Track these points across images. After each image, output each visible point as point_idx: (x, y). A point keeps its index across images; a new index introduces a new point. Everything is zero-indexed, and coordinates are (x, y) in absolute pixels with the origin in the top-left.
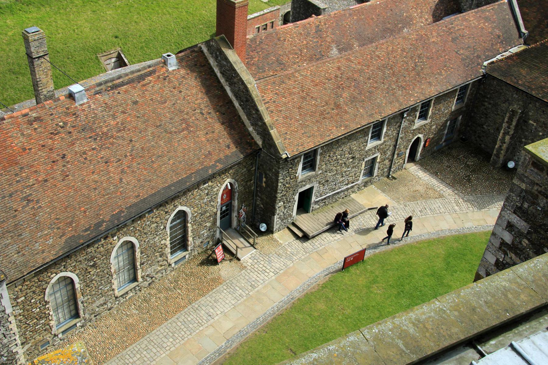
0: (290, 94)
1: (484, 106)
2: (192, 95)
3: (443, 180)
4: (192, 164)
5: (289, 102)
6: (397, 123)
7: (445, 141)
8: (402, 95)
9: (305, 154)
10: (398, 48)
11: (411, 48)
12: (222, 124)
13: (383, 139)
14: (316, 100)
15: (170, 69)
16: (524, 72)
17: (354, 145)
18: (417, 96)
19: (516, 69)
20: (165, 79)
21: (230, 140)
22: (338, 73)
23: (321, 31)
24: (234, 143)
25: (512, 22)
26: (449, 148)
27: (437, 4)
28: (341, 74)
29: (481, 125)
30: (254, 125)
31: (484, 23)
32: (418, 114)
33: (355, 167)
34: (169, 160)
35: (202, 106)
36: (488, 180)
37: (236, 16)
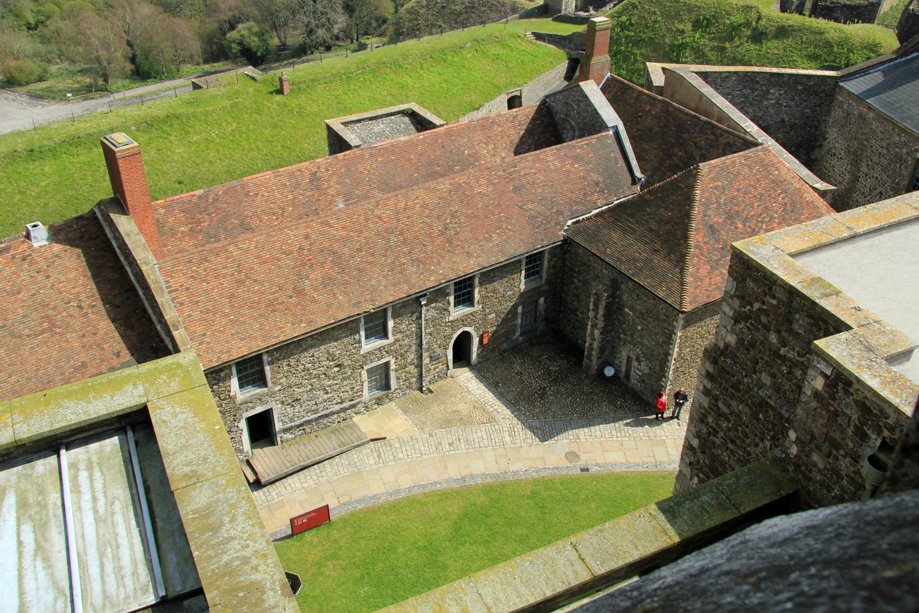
0: (217, 277)
1: (574, 283)
2: (69, 280)
3: (501, 396)
4: (49, 382)
5: (213, 289)
6: (413, 313)
7: (521, 335)
8: (416, 273)
9: (238, 364)
10: (416, 204)
11: (439, 203)
12: (113, 322)
13: (391, 339)
14: (261, 283)
15: (36, 245)
16: (615, 236)
17: (335, 347)
18: (442, 274)
19: (605, 231)
20: (24, 260)
21: (123, 345)
22: (306, 244)
23: (319, 180)
24: (129, 349)
25: (621, 162)
26: (531, 345)
27: (523, 137)
28: (311, 245)
29: (574, 311)
30: (160, 322)
32: (452, 299)
33: (349, 378)
34: (10, 376)
35: (83, 297)
36: (568, 395)
37: (121, 169)
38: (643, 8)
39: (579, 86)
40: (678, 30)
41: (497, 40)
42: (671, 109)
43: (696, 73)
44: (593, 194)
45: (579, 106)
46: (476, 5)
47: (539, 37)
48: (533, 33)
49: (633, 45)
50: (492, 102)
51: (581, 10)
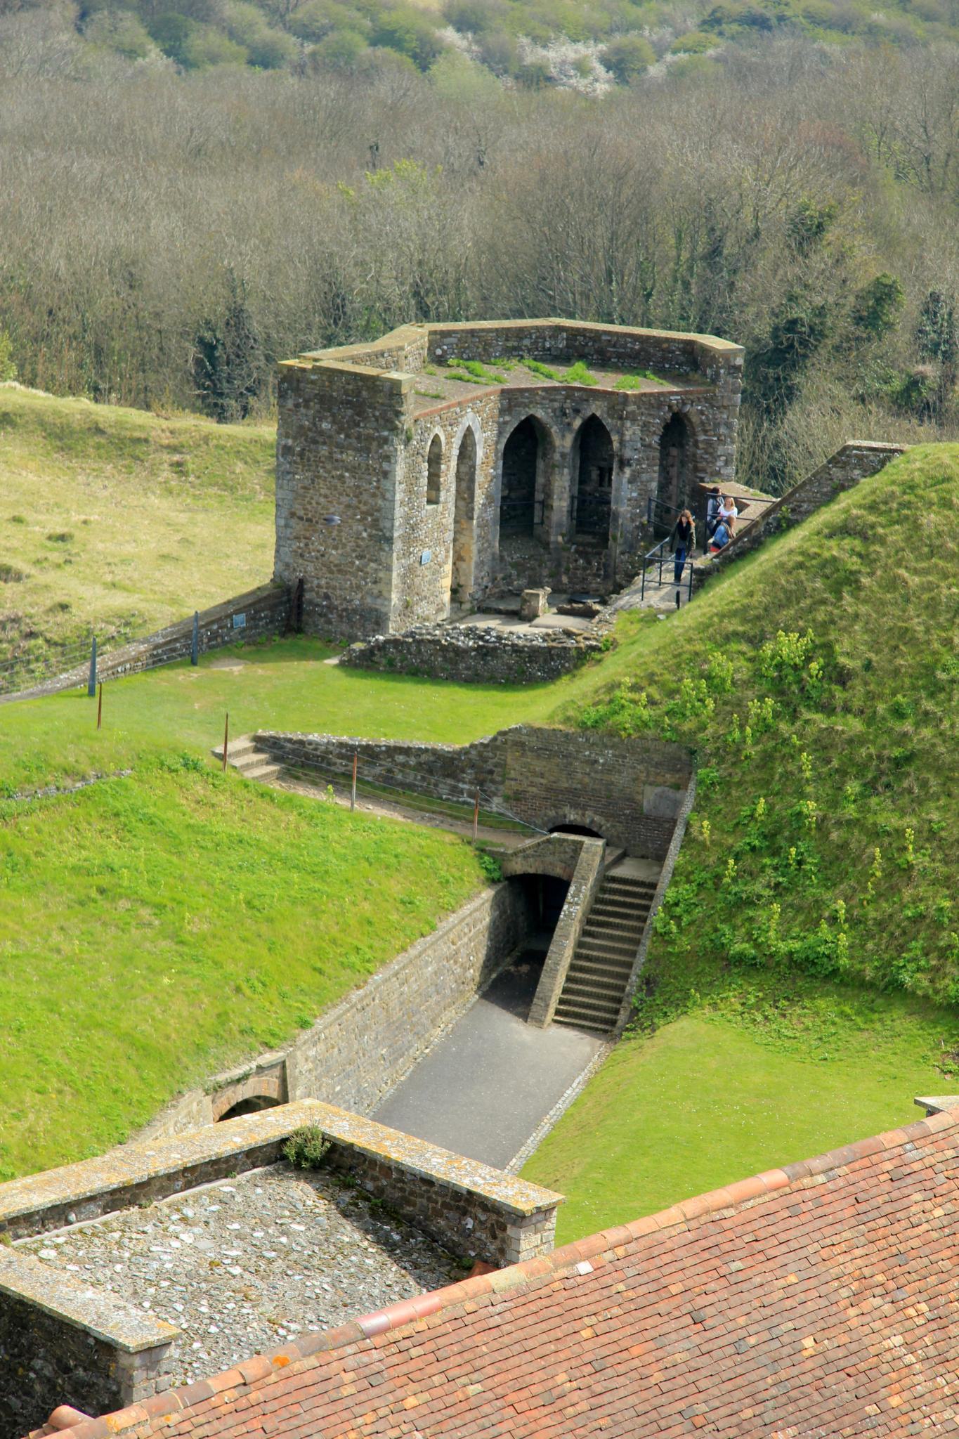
38: (892, 584)
47: (298, 760)
49: (871, 787)
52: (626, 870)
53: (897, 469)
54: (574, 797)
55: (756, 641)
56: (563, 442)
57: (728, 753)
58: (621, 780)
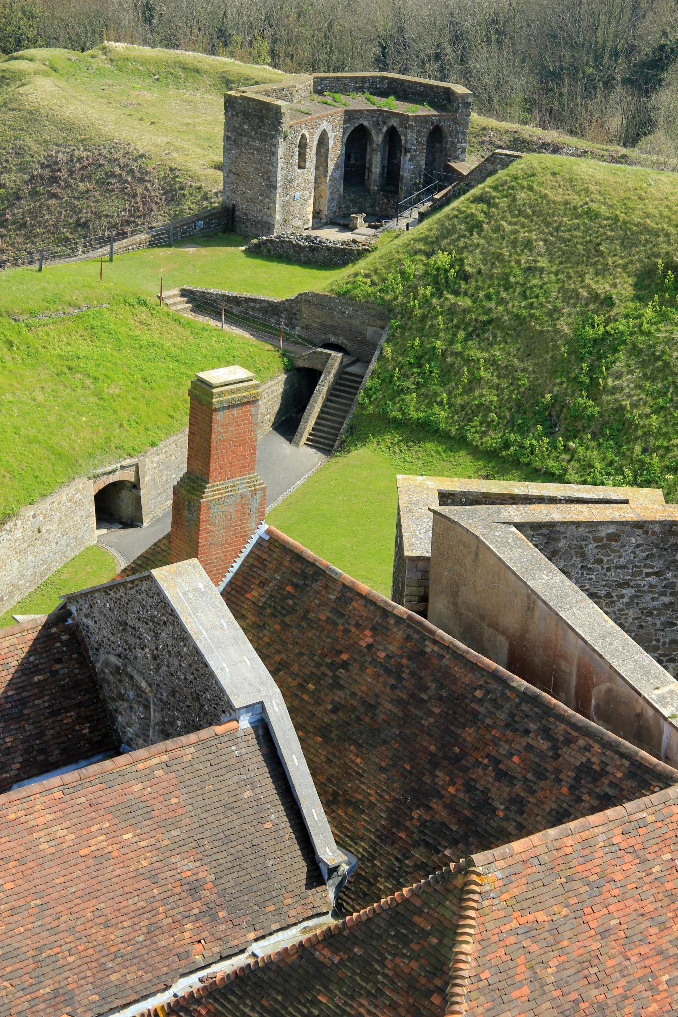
25: (277, 815)
31: (112, 834)
38: (498, 229)
39: (150, 578)
40: (594, 297)
41: (78, 314)
42: (429, 648)
43: (519, 526)
44: (178, 924)
45: (156, 637)
46: (64, 174)
47: (201, 303)
48: (185, 293)
49: (469, 336)
50: (46, 504)
51: (332, 223)
52: (352, 369)
53: (515, 167)
54: (334, 329)
55: (428, 255)
56: (378, 138)
57: (407, 313)
58: (356, 322)
